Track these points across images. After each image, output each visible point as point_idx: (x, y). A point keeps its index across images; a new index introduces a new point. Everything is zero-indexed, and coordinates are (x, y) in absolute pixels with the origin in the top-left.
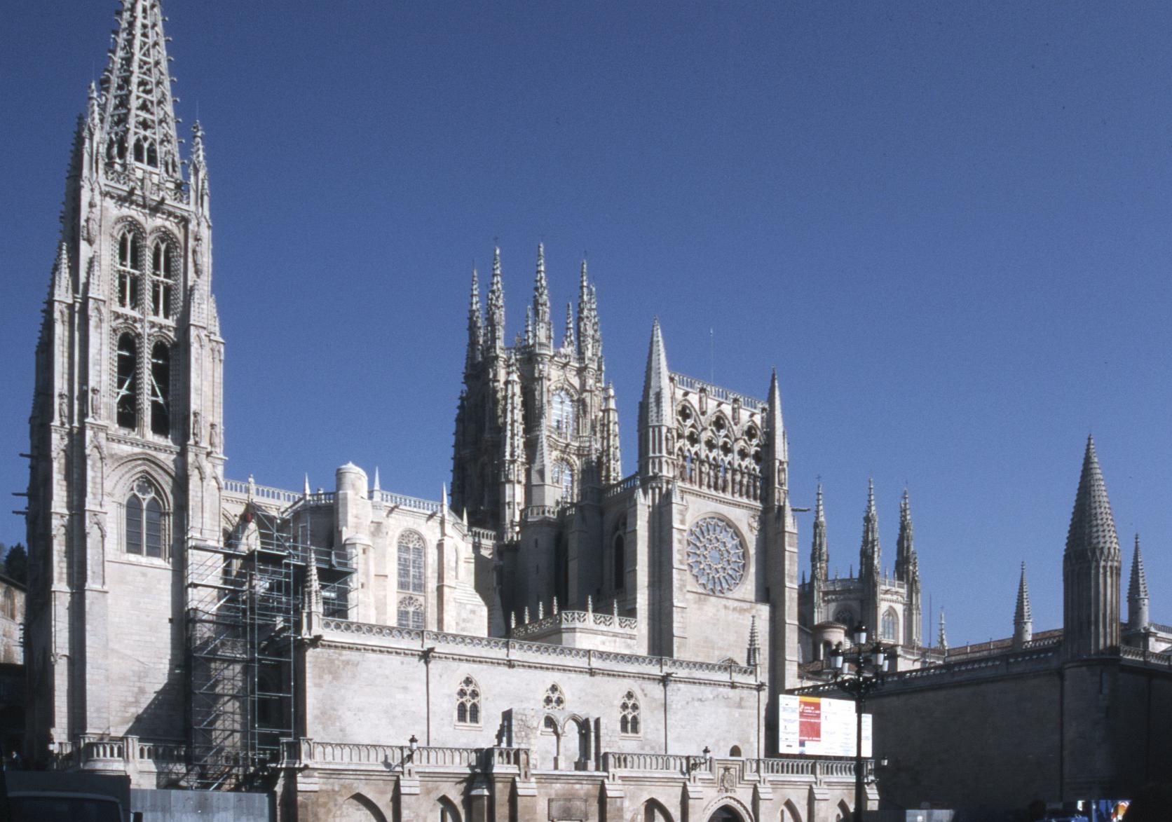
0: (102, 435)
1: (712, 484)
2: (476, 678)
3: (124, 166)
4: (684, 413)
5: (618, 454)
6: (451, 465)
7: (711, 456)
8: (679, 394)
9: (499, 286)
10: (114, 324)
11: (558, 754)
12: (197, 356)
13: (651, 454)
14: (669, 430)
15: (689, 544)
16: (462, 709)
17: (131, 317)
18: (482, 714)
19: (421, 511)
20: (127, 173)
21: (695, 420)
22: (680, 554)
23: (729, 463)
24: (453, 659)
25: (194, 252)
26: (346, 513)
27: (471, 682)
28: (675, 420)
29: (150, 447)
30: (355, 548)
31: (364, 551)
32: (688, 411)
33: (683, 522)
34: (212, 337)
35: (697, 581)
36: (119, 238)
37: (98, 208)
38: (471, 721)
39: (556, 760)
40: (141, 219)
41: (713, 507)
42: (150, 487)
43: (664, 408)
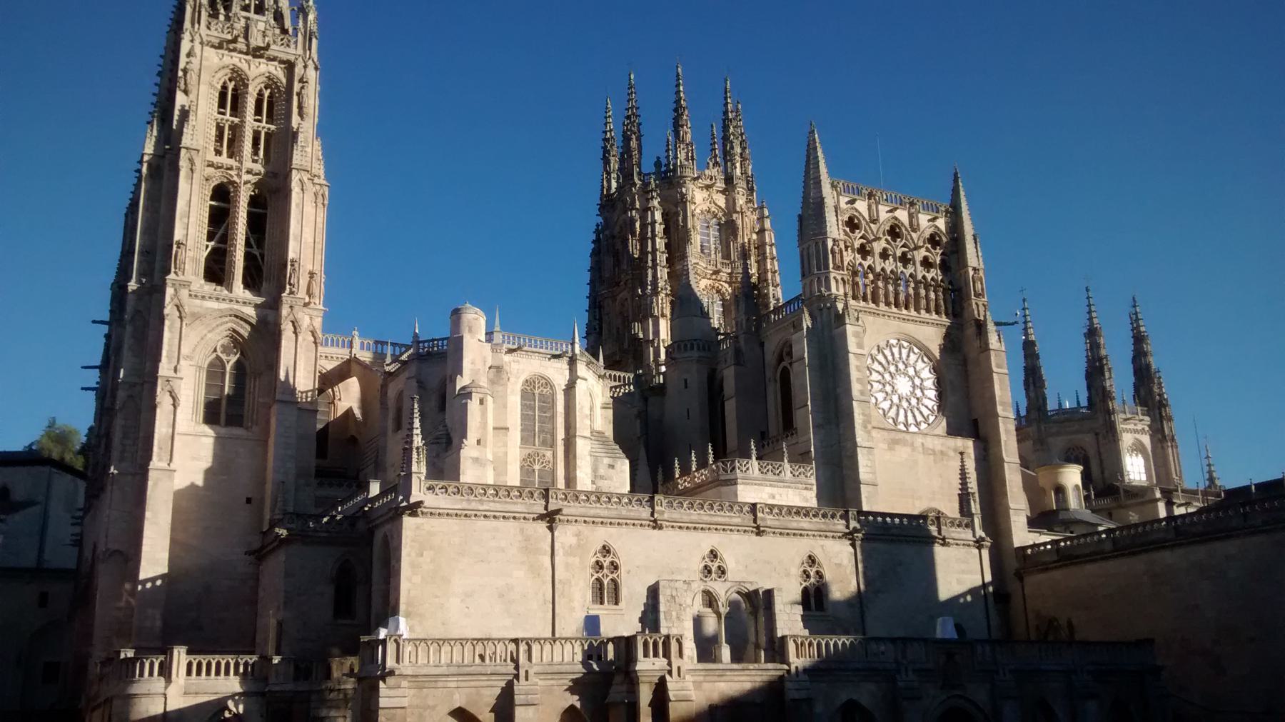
0: (184, 293)
1: (892, 300)
2: (615, 545)
3: (228, 18)
4: (852, 224)
5: (778, 279)
6: (586, 304)
12: (298, 201)
14: (834, 240)
16: (599, 587)
18: (624, 592)
20: (231, 22)
21: (866, 230)
25: (299, 94)
28: (841, 231)
29: (237, 302)
31: (482, 402)
32: (856, 221)
33: (860, 346)
34: (316, 180)
36: (219, 87)
37: (199, 58)
40: (244, 66)
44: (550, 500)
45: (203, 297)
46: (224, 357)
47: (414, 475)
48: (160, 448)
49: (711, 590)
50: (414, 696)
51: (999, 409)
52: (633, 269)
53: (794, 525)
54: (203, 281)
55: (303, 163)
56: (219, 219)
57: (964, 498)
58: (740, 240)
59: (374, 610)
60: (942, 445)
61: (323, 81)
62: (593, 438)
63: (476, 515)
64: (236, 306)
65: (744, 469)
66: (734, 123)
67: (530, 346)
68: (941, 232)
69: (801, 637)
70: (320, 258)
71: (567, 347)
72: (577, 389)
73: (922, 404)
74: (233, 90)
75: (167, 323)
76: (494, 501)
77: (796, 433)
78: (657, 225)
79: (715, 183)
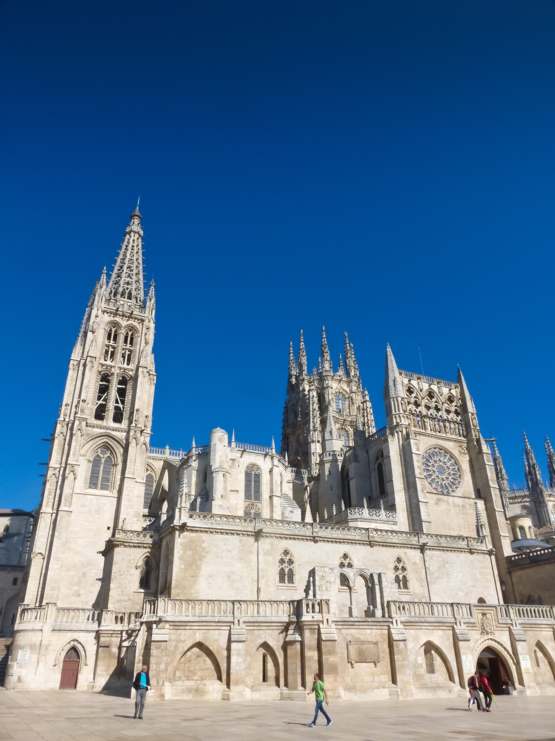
2: (292, 550)
4: (410, 391)
7: (429, 413)
8: (406, 381)
9: (303, 346)
10: (100, 369)
11: (351, 605)
13: (394, 413)
14: (402, 399)
15: (423, 464)
16: (282, 574)
17: (109, 366)
18: (296, 578)
19: (262, 452)
21: (417, 394)
22: (420, 469)
23: (441, 416)
24: (276, 537)
26: (215, 455)
27: (288, 553)
28: (405, 394)
30: (219, 474)
32: (412, 390)
33: (418, 449)
35: (432, 486)
38: (289, 582)
39: (350, 609)
41: (433, 442)
42: (107, 451)
43: (398, 388)
44: (256, 524)
45: (94, 427)
46: (101, 456)
47: (182, 509)
48: (66, 500)
49: (345, 573)
50: (173, 634)
51: (491, 483)
52: (303, 419)
53: (390, 541)
54: (94, 419)
55: (145, 364)
56: (103, 390)
57: (479, 528)
58: (355, 405)
59: (160, 585)
60: (463, 501)
61: (156, 328)
62: (282, 497)
63: (216, 532)
64: (109, 431)
65: (361, 513)
66: (350, 352)
67: (250, 449)
68: (453, 395)
69: (398, 602)
70: (151, 409)
71: (269, 450)
72: (274, 471)
73: (450, 481)
74: (115, 332)
75: (74, 438)
76: (225, 524)
77: (387, 496)
78: (315, 398)
79: (342, 378)
